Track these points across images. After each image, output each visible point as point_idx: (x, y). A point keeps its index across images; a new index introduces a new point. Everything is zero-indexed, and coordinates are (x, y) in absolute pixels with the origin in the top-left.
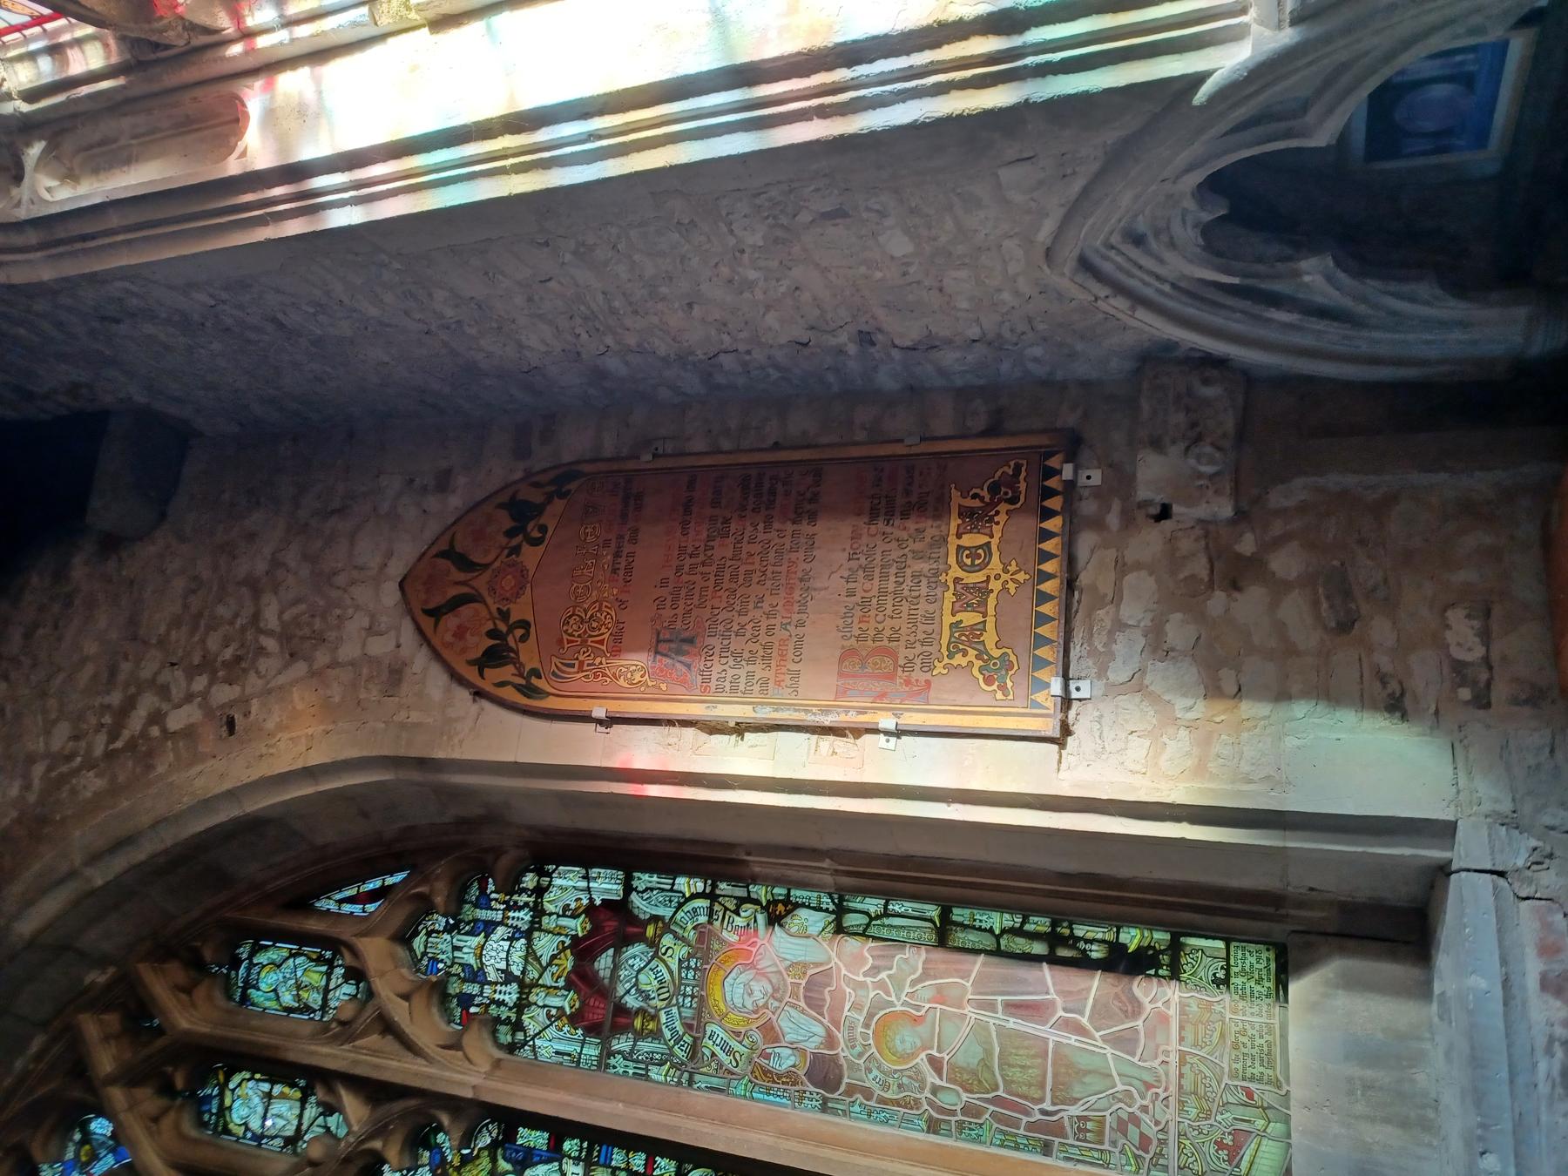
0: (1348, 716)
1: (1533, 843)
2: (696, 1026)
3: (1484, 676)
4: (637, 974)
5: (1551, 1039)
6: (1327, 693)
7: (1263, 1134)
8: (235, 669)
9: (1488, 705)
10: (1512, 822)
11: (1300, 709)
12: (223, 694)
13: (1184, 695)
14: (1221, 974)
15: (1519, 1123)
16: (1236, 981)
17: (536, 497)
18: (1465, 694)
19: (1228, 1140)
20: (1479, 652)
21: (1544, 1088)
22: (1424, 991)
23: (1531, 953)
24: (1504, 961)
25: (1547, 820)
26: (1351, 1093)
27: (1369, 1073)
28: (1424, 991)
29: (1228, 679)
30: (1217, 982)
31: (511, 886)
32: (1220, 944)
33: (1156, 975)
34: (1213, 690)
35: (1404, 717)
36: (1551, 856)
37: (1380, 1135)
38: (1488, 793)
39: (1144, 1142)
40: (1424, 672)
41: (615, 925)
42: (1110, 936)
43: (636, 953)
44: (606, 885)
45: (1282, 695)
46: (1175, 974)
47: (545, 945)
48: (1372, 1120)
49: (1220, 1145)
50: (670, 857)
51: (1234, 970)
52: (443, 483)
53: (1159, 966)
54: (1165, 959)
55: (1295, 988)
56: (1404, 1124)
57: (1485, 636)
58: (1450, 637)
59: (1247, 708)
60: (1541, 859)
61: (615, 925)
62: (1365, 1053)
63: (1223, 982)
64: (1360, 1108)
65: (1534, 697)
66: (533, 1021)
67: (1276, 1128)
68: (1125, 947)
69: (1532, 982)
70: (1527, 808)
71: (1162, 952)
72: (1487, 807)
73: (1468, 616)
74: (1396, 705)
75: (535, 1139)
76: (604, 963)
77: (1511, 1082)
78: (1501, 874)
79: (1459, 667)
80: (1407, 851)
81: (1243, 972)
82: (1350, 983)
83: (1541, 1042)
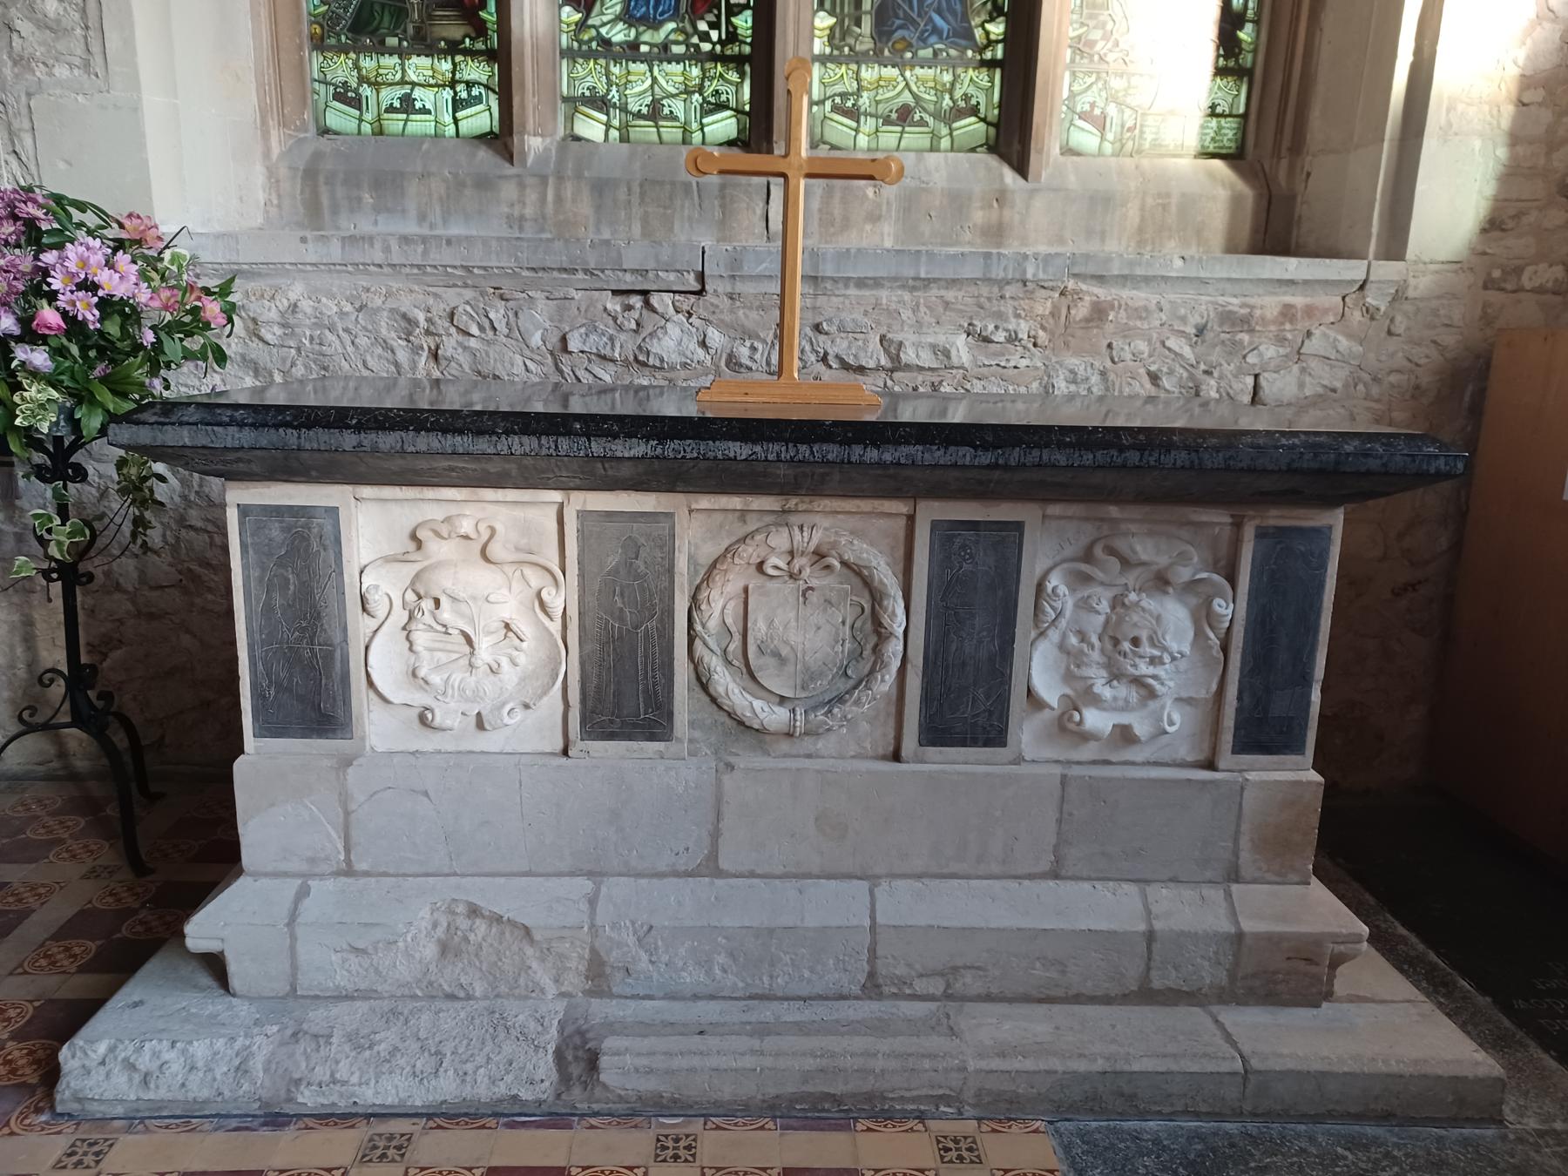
0: (1490, 189)
1: (1383, 309)
3: (1509, 287)
5: (1252, 307)
6: (1512, 174)
7: (1103, 138)
9: (1485, 287)
10: (1399, 296)
11: (1502, 153)
13: (1528, 58)
14: (1219, 110)
15: (1204, 282)
16: (1214, 122)
18: (1497, 274)
19: (1097, 112)
20: (1527, 284)
21: (1221, 300)
22: (1231, 248)
23: (1308, 300)
24: (1306, 282)
25: (1399, 318)
26: (1159, 195)
27: (1174, 209)
28: (1231, 248)
29: (1536, 95)
30: (1213, 107)
32: (1242, 110)
33: (1218, 56)
34: (1527, 82)
35: (1484, 231)
36: (1372, 318)
37: (1133, 213)
38: (1421, 285)
39: (1092, 44)
40: (1517, 245)
42: (1250, 14)
45: (1515, 138)
46: (1220, 72)
48: (1142, 209)
49: (1093, 105)
51: (1223, 121)
53: (1226, 57)
54: (1231, 63)
55: (1217, 163)
56: (1141, 230)
57: (1540, 290)
58: (1543, 266)
59: (1508, 110)
60: (1371, 314)
62: (1188, 203)
63: (1213, 112)
64: (1150, 201)
65: (1487, 319)
67: (1108, 148)
68: (1241, 28)
69: (1288, 299)
70: (1408, 307)
71: (1237, 61)
72: (1412, 282)
73: (1556, 280)
74: (1493, 225)
77: (1229, 279)
78: (1362, 288)
79: (1518, 271)
80: (1375, 230)
81: (1220, 128)
82: (1236, 201)
83: (1251, 301)
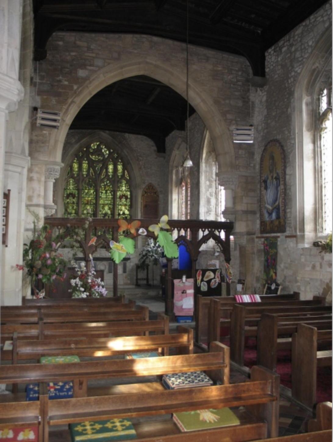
2: (121, 205)
4: (123, 200)
8: (144, 167)
12: (143, 167)
17: (157, 194)
31: (128, 188)
41: (126, 198)
43: (125, 200)
44: (129, 196)
47: (125, 192)
50: (131, 202)
52: (158, 185)
61: (126, 198)
66: (120, 192)
75: (112, 193)
76: (124, 197)
